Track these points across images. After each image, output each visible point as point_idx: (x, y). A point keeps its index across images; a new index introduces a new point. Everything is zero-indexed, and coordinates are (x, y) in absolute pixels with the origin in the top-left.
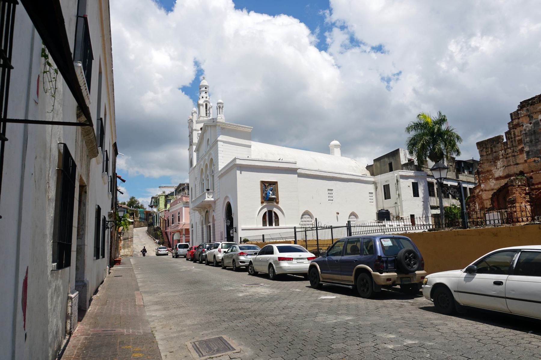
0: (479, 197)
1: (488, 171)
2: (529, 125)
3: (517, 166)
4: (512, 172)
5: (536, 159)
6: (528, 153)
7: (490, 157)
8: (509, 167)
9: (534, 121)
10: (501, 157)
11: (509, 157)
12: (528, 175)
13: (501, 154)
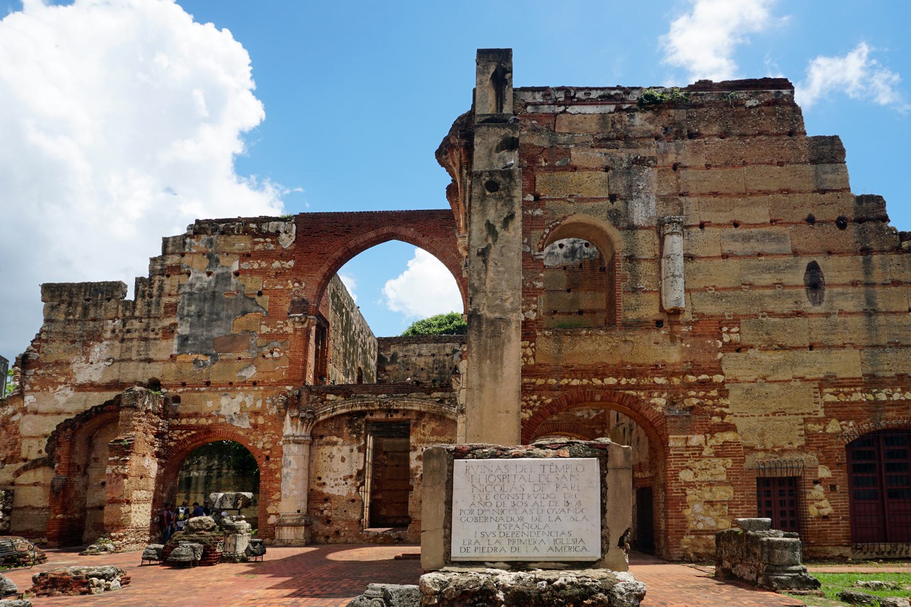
1: (57, 363)
3: (148, 365)
4: (130, 378)
5: (201, 357)
8: (123, 364)
12: (171, 391)
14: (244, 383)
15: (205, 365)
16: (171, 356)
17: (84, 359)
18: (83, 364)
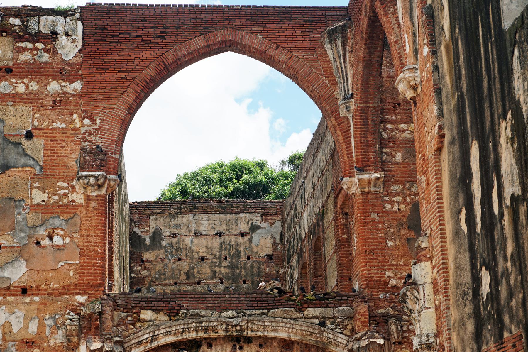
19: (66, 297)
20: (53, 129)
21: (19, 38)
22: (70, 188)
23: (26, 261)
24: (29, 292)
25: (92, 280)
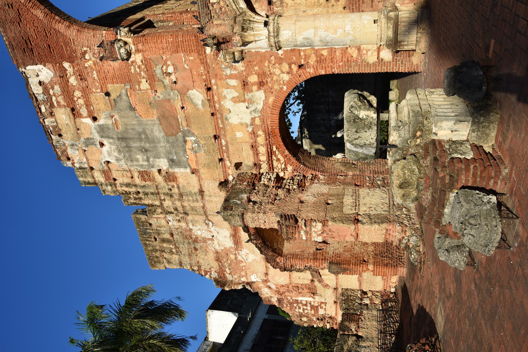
0: (282, 290)
2: (105, 149)
3: (206, 193)
5: (189, 146)
6: (172, 162)
7: (184, 248)
9: (97, 138)
10: (183, 225)
11: (183, 207)
12: (230, 172)
13: (176, 224)
14: (210, 101)
15: (196, 142)
16: (193, 173)
17: (210, 242)
18: (216, 242)
19: (208, 61)
20: (99, 79)
21: (52, 106)
22: (134, 64)
23: (188, 90)
24: (209, 86)
25: (193, 43)
